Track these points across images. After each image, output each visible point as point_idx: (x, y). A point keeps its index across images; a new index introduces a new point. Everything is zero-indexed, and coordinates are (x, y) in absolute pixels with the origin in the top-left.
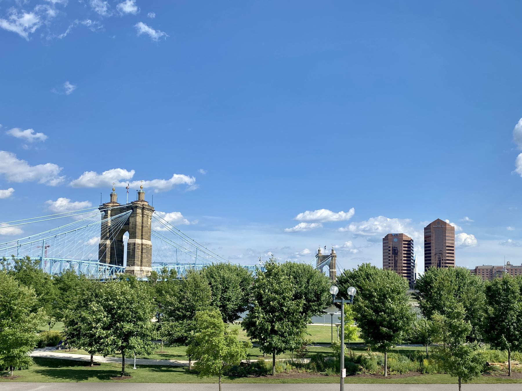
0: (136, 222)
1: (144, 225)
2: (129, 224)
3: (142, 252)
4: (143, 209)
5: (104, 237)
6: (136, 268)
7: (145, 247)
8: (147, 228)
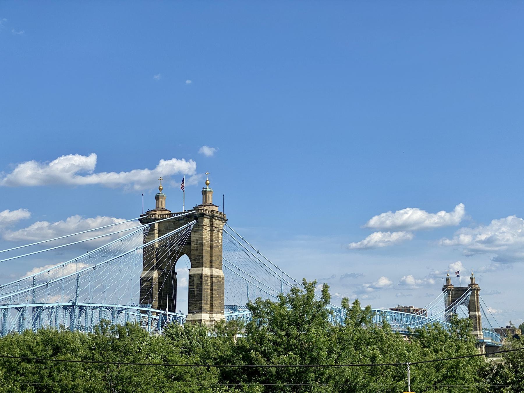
0: (202, 239)
1: (214, 244)
3: (212, 290)
4: (212, 217)
5: (147, 265)
6: (205, 317)
8: (217, 249)
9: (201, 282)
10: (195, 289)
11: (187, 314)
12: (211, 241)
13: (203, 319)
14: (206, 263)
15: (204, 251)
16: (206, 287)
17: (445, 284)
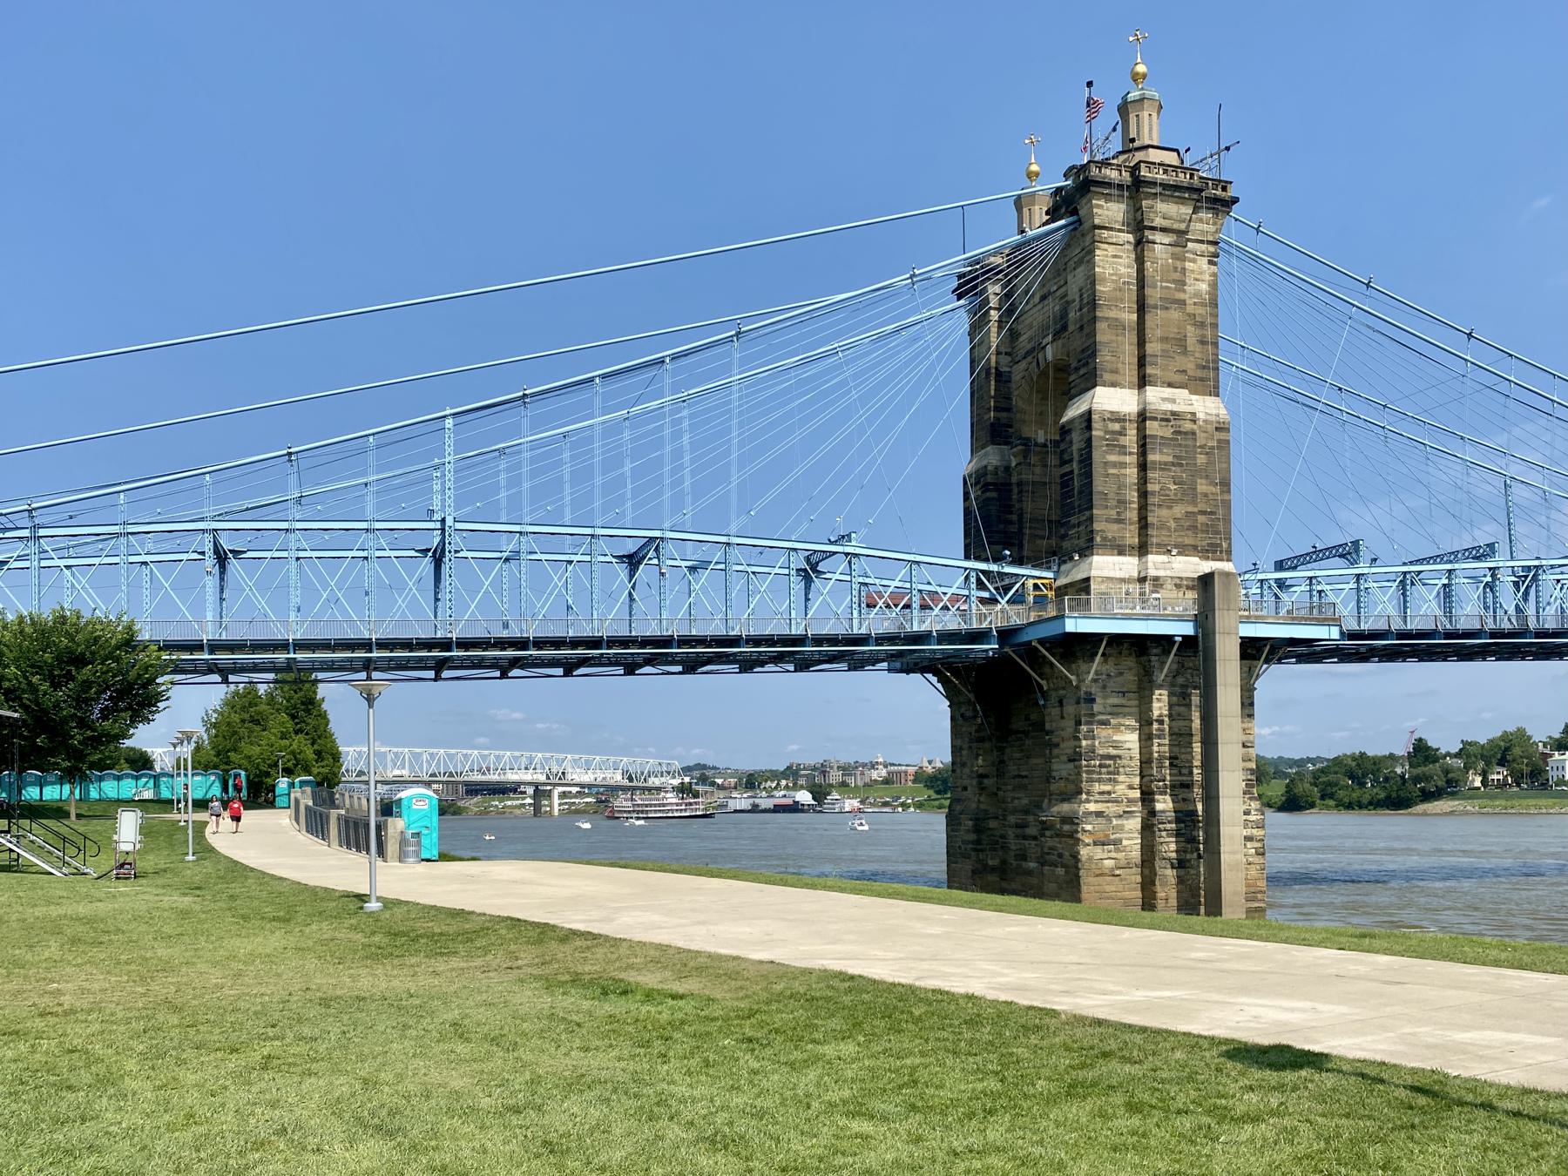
1: (1153, 295)
3: (1143, 467)
8: (1175, 314)
9: (1089, 441)
10: (1076, 472)
13: (1094, 573)
14: (1116, 372)
15: (1101, 326)
16: (1112, 458)
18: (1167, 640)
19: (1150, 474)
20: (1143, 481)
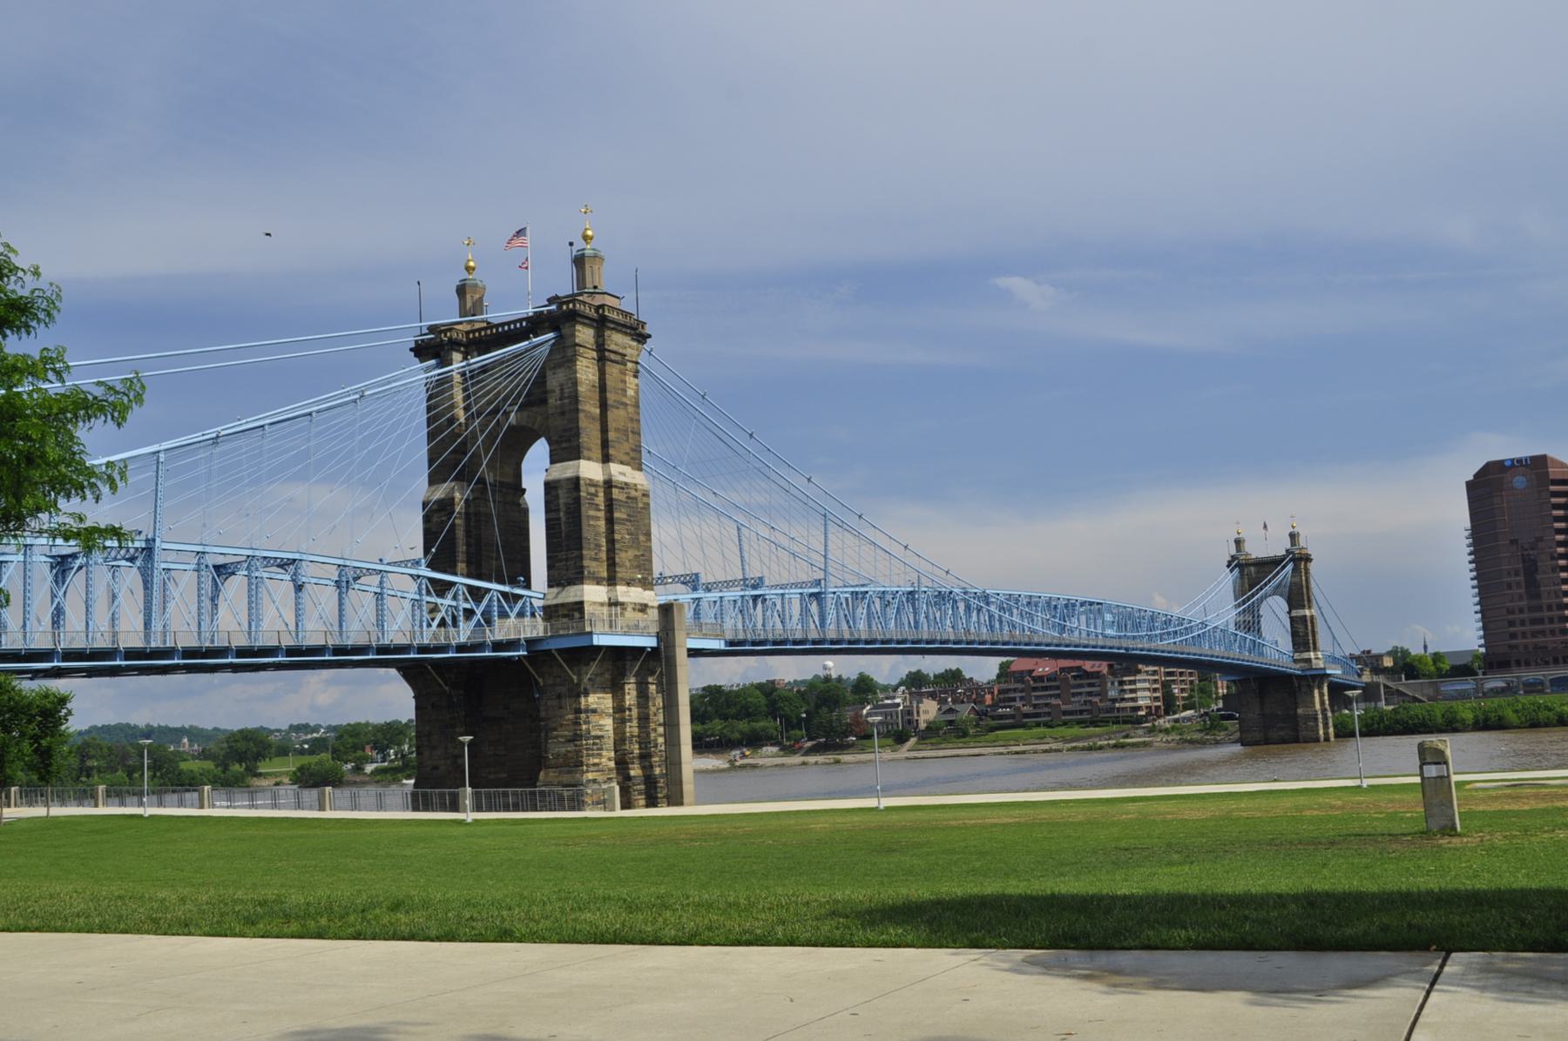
0: (575, 383)
2: (544, 401)
3: (610, 521)
6: (593, 594)
7: (622, 497)
8: (622, 412)
9: (578, 500)
11: (546, 590)
12: (603, 388)
13: (586, 598)
15: (581, 415)
16: (592, 513)
17: (1233, 552)
18: (642, 649)
19: (616, 527)
20: (610, 531)
